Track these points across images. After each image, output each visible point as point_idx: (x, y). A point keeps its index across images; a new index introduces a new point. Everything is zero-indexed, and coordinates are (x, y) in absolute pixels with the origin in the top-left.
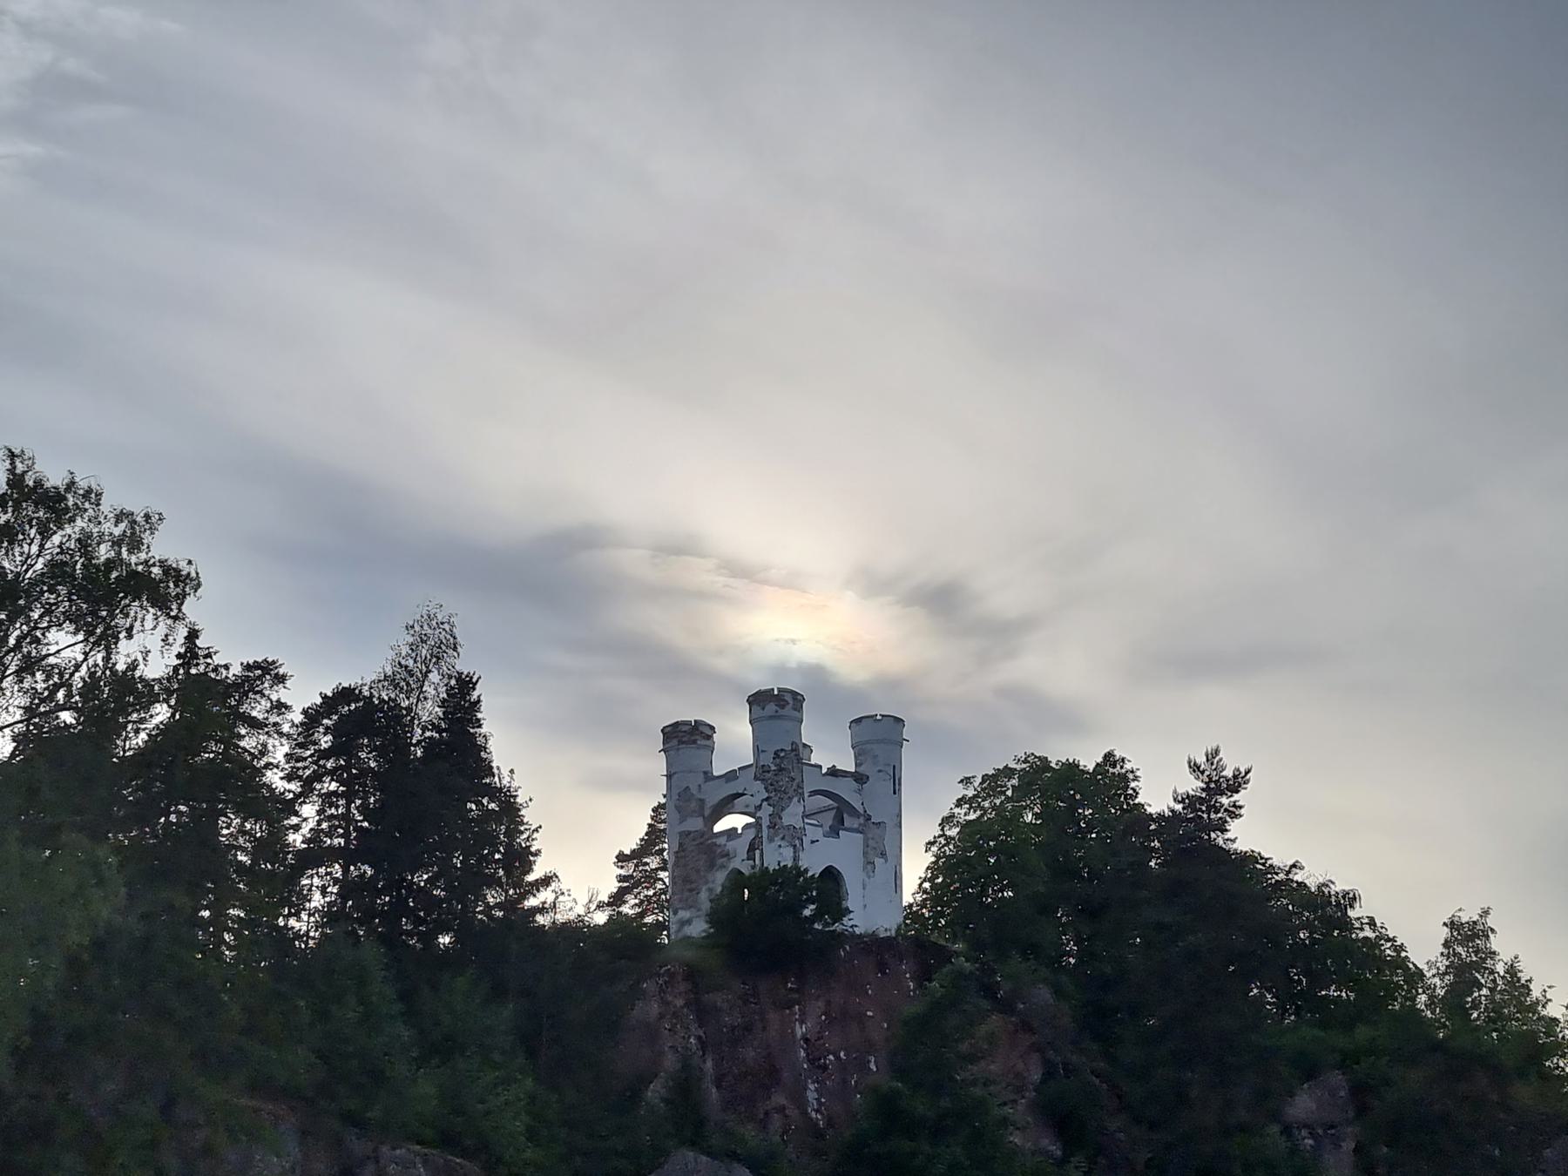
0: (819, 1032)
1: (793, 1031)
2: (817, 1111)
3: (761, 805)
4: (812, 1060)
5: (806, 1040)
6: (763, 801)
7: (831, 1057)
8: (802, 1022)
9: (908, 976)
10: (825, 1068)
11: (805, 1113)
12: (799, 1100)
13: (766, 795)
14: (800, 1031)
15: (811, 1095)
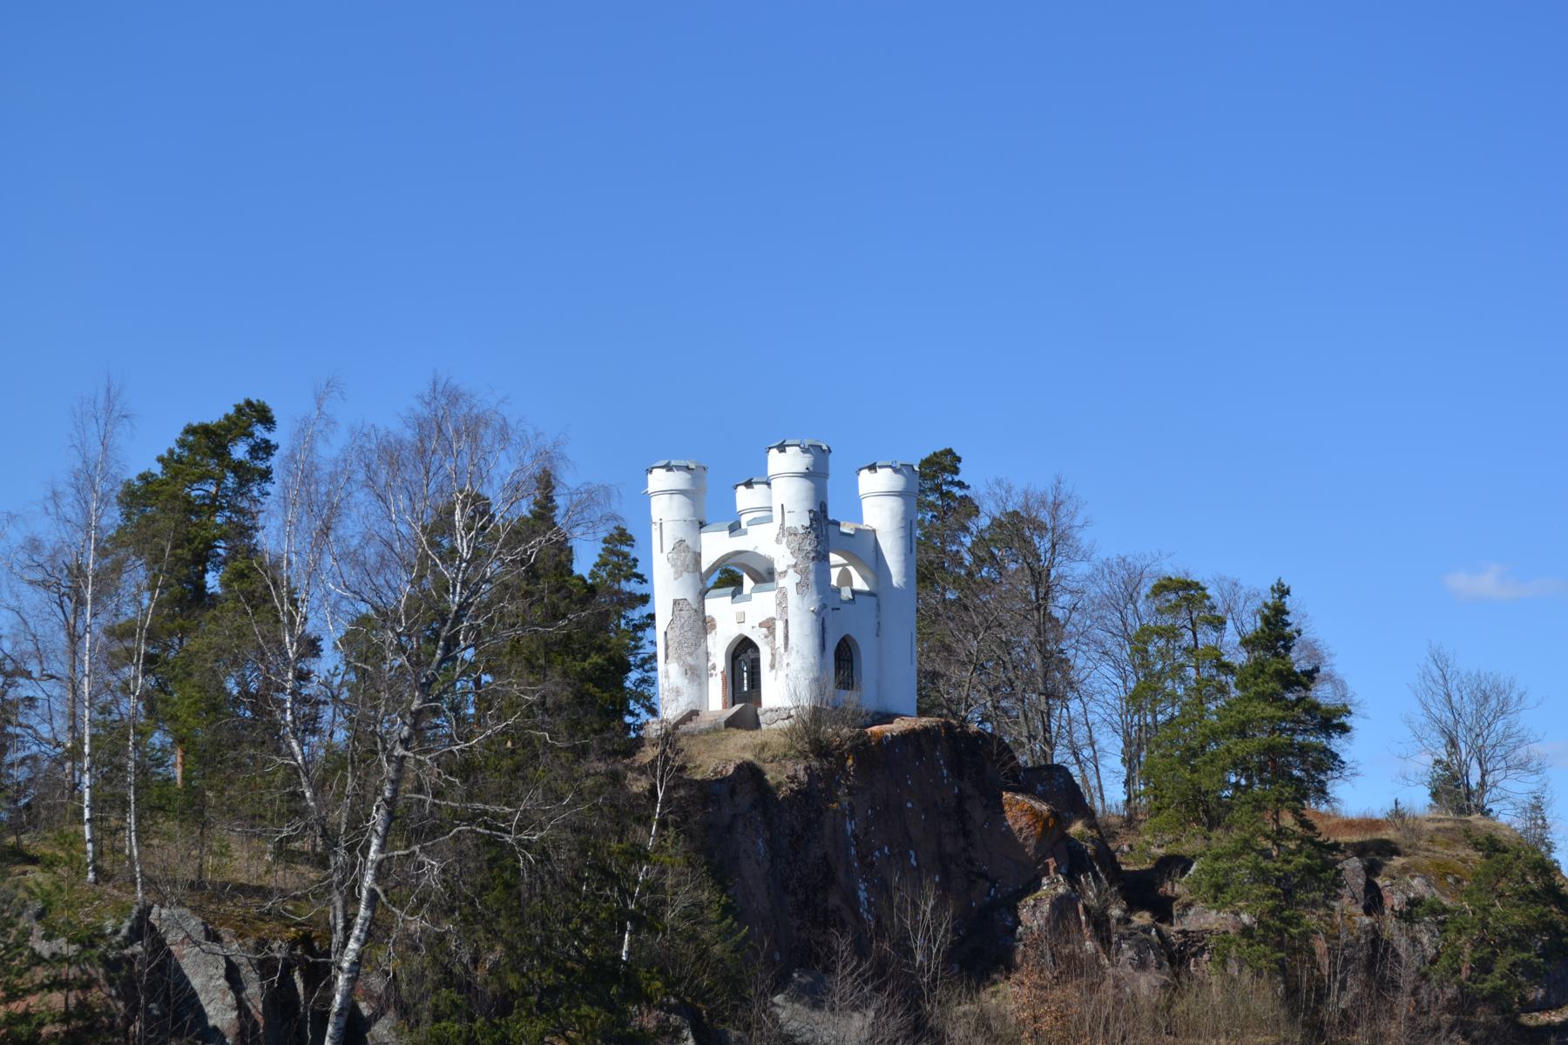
0: (866, 828)
1: (845, 830)
2: (869, 911)
3: (786, 572)
4: (862, 858)
5: (856, 837)
6: (789, 567)
7: (877, 853)
8: (852, 819)
9: (941, 762)
10: (872, 864)
11: (857, 915)
12: (851, 899)
13: (793, 561)
14: (849, 828)
15: (862, 895)
